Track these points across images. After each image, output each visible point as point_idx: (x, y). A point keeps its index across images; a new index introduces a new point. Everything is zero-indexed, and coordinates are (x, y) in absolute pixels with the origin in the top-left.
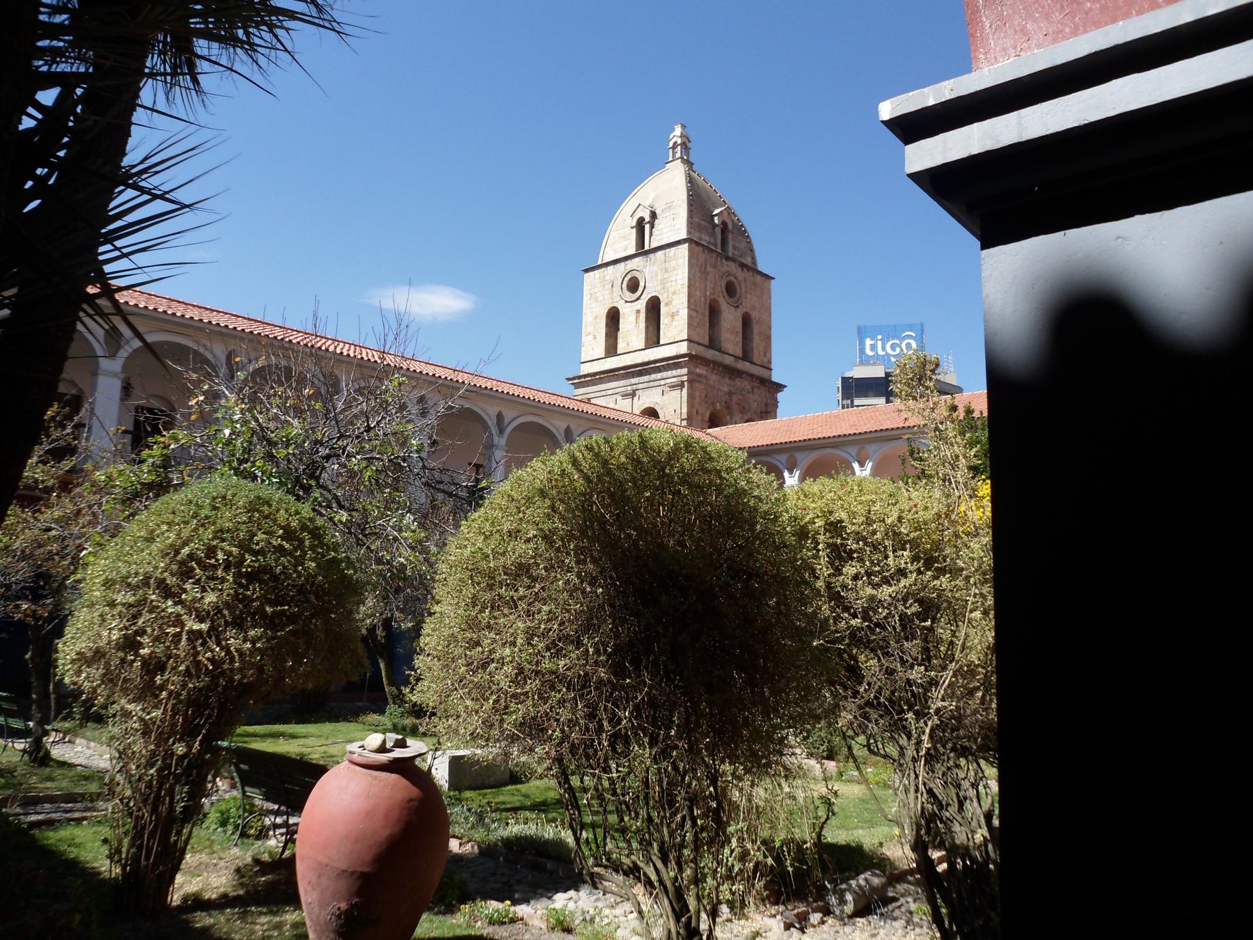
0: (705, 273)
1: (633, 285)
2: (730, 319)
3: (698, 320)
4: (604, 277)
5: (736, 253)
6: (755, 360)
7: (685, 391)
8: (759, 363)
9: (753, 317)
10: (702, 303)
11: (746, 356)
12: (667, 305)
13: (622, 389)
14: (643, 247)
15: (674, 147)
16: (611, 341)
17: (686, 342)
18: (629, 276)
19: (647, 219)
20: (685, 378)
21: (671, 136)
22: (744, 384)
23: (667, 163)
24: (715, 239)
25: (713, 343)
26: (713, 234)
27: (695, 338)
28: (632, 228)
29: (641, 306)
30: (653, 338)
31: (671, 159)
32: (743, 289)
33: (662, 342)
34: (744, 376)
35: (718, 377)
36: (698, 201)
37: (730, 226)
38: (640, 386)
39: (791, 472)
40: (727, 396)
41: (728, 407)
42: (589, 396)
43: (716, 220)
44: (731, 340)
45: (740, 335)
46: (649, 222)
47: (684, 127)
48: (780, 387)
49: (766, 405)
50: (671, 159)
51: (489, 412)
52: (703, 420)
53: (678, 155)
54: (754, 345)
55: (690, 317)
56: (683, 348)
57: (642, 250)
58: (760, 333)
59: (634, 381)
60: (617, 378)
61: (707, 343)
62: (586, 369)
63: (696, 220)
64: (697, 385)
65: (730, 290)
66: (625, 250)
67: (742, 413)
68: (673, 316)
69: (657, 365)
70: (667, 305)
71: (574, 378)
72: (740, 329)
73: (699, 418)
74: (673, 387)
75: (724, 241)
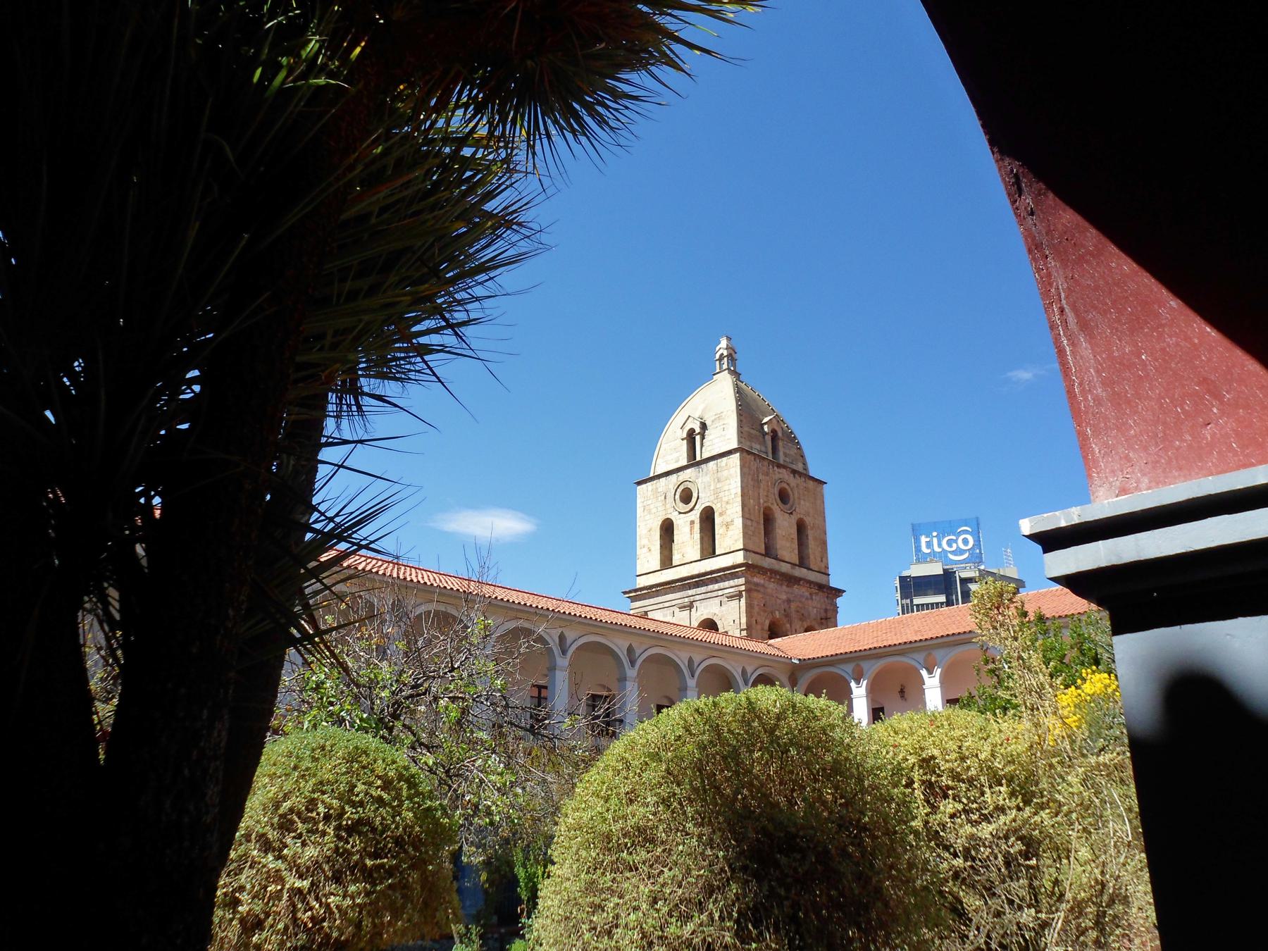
1: (686, 497)
4: (657, 489)
5: (787, 460)
6: (812, 567)
7: (743, 600)
10: (757, 511)
11: (803, 562)
13: (679, 601)
15: (721, 358)
16: (666, 553)
17: (742, 552)
18: (682, 488)
19: (698, 430)
20: (743, 588)
21: (717, 349)
23: (714, 374)
24: (766, 447)
26: (764, 443)
27: (750, 547)
28: (683, 439)
29: (695, 516)
30: (709, 549)
32: (796, 495)
33: (717, 552)
34: (801, 582)
35: (775, 585)
36: (747, 411)
37: (780, 434)
38: (698, 598)
39: (858, 682)
40: (786, 604)
42: (646, 609)
43: (766, 428)
44: (787, 547)
45: (796, 541)
46: (699, 433)
47: (729, 339)
48: (839, 592)
49: (826, 611)
50: (718, 370)
52: (762, 629)
53: (725, 366)
54: (810, 550)
55: (745, 526)
56: (739, 558)
57: (694, 462)
58: (815, 539)
59: (691, 592)
60: (674, 590)
61: (763, 552)
62: (642, 582)
63: (746, 429)
64: (755, 594)
65: (783, 497)
66: (677, 461)
67: (801, 619)
68: (727, 525)
70: (721, 514)
71: (630, 592)
72: (795, 536)
73: (759, 627)
74: (731, 597)
75: (775, 449)
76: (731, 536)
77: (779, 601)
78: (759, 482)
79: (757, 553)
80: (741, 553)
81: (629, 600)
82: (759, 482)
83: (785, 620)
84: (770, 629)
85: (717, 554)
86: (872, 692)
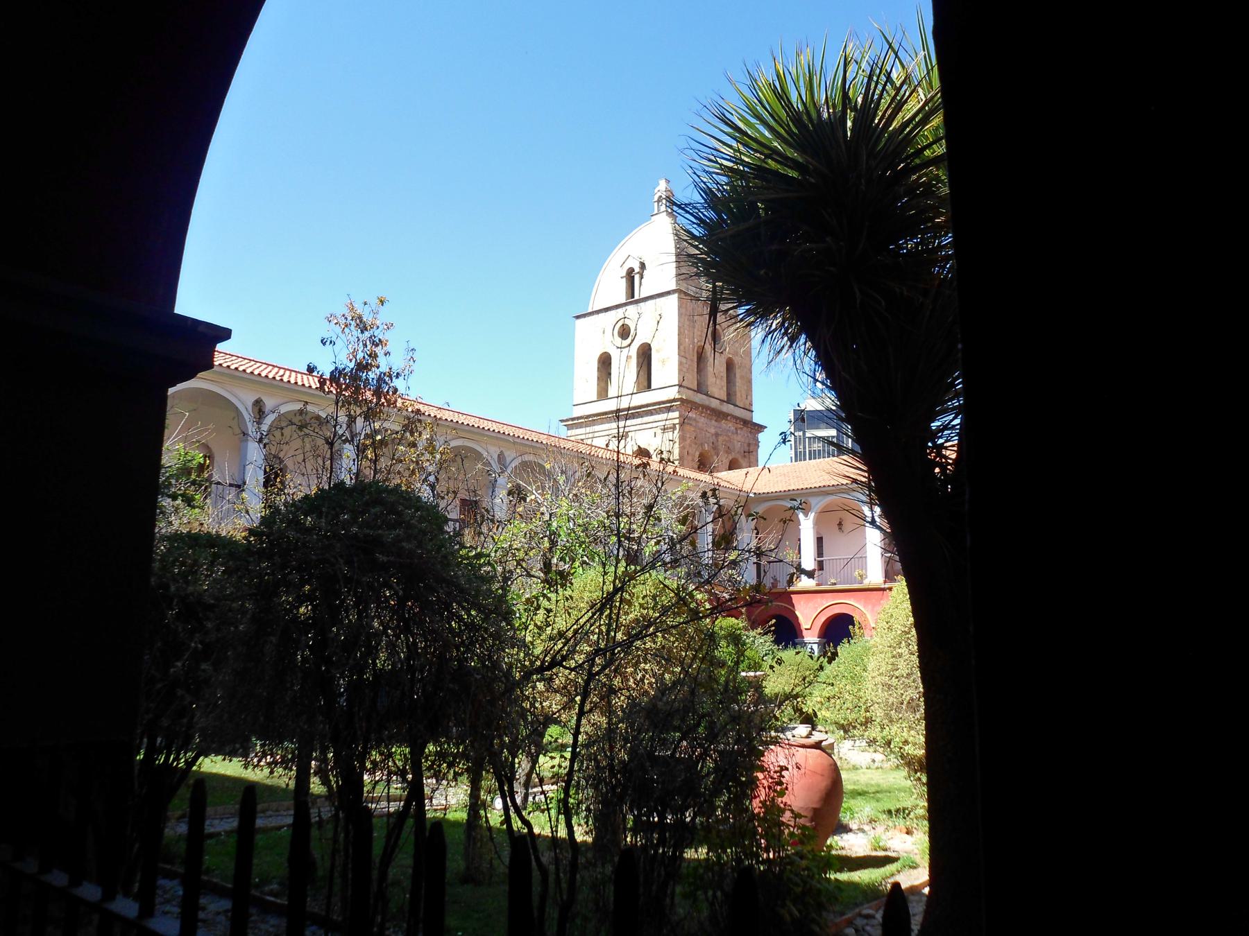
1: (625, 332)
2: (716, 367)
3: (687, 366)
6: (738, 404)
9: (736, 362)
11: (730, 399)
12: (658, 351)
14: (633, 297)
15: (659, 201)
16: (603, 384)
18: (620, 324)
19: (637, 270)
20: (677, 421)
21: (656, 191)
22: (729, 425)
23: (652, 216)
25: (701, 388)
28: (622, 278)
29: (633, 351)
31: (656, 212)
34: (729, 418)
35: (706, 419)
39: (806, 515)
40: (714, 437)
41: (715, 448)
44: (717, 386)
46: (638, 273)
47: (668, 181)
48: (761, 428)
49: (749, 445)
50: (656, 212)
51: (490, 452)
52: (693, 460)
54: (737, 388)
55: (680, 364)
56: (673, 393)
58: (742, 377)
62: (578, 412)
64: (687, 427)
71: (567, 420)
73: (690, 458)
76: (667, 371)
77: (708, 435)
79: (691, 389)
80: (677, 387)
81: (566, 428)
83: (713, 452)
84: (731, 462)
85: (652, 388)
86: (817, 523)
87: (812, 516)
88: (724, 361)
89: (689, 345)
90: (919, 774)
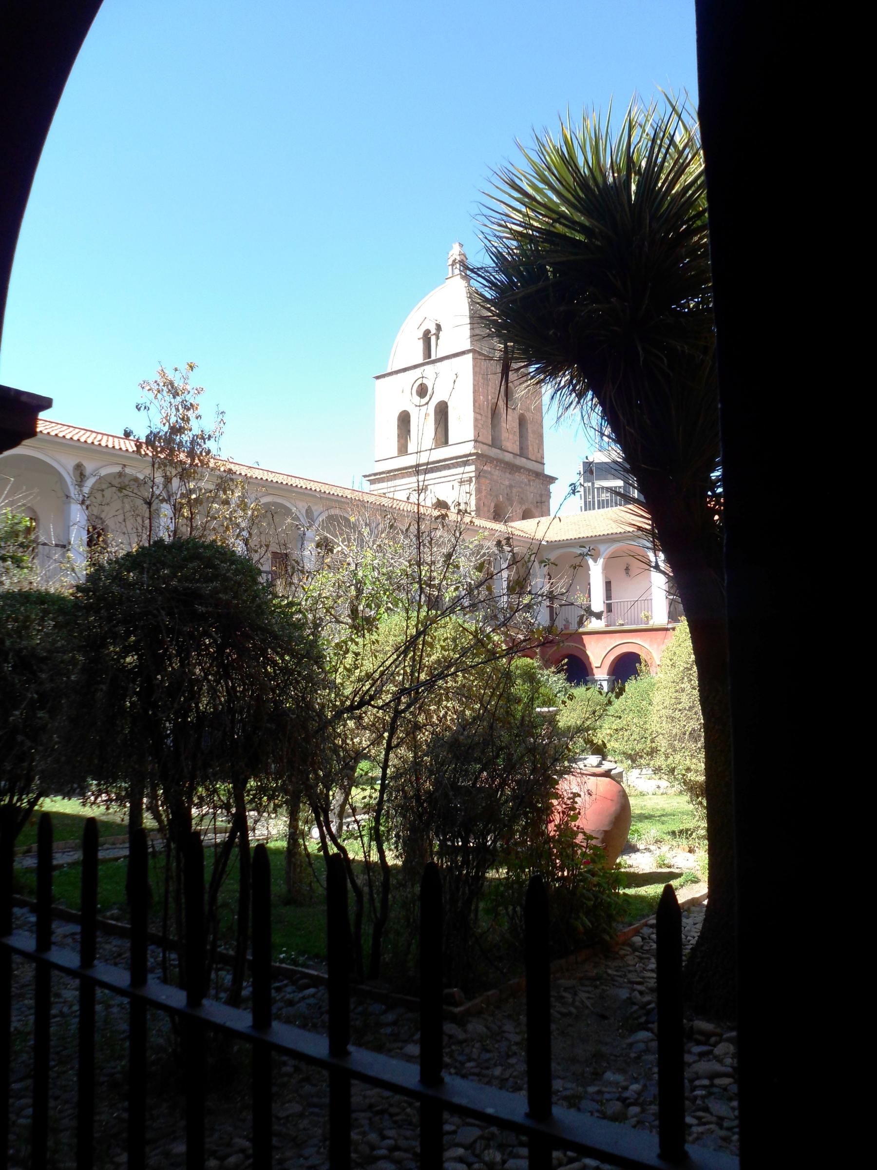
0: (486, 380)
1: (422, 391)
6: (530, 456)
7: (473, 484)
8: (534, 459)
11: (523, 452)
14: (430, 357)
16: (403, 441)
20: (473, 474)
21: (450, 255)
25: (495, 443)
27: (480, 439)
31: (450, 275)
34: (522, 470)
39: (595, 561)
40: (508, 489)
41: (509, 499)
42: (385, 491)
44: (511, 442)
45: (518, 434)
46: (434, 334)
47: (461, 245)
48: (552, 479)
49: (541, 496)
50: (450, 275)
51: (298, 508)
52: (489, 511)
55: (476, 420)
56: (469, 448)
58: (534, 432)
61: (490, 443)
64: (483, 480)
69: (447, 463)
72: (517, 429)
73: (486, 509)
78: (488, 380)
80: (473, 442)
82: (488, 380)
85: (450, 443)
86: (606, 568)
87: (601, 561)
88: (517, 417)
89: (484, 402)
90: (700, 798)
